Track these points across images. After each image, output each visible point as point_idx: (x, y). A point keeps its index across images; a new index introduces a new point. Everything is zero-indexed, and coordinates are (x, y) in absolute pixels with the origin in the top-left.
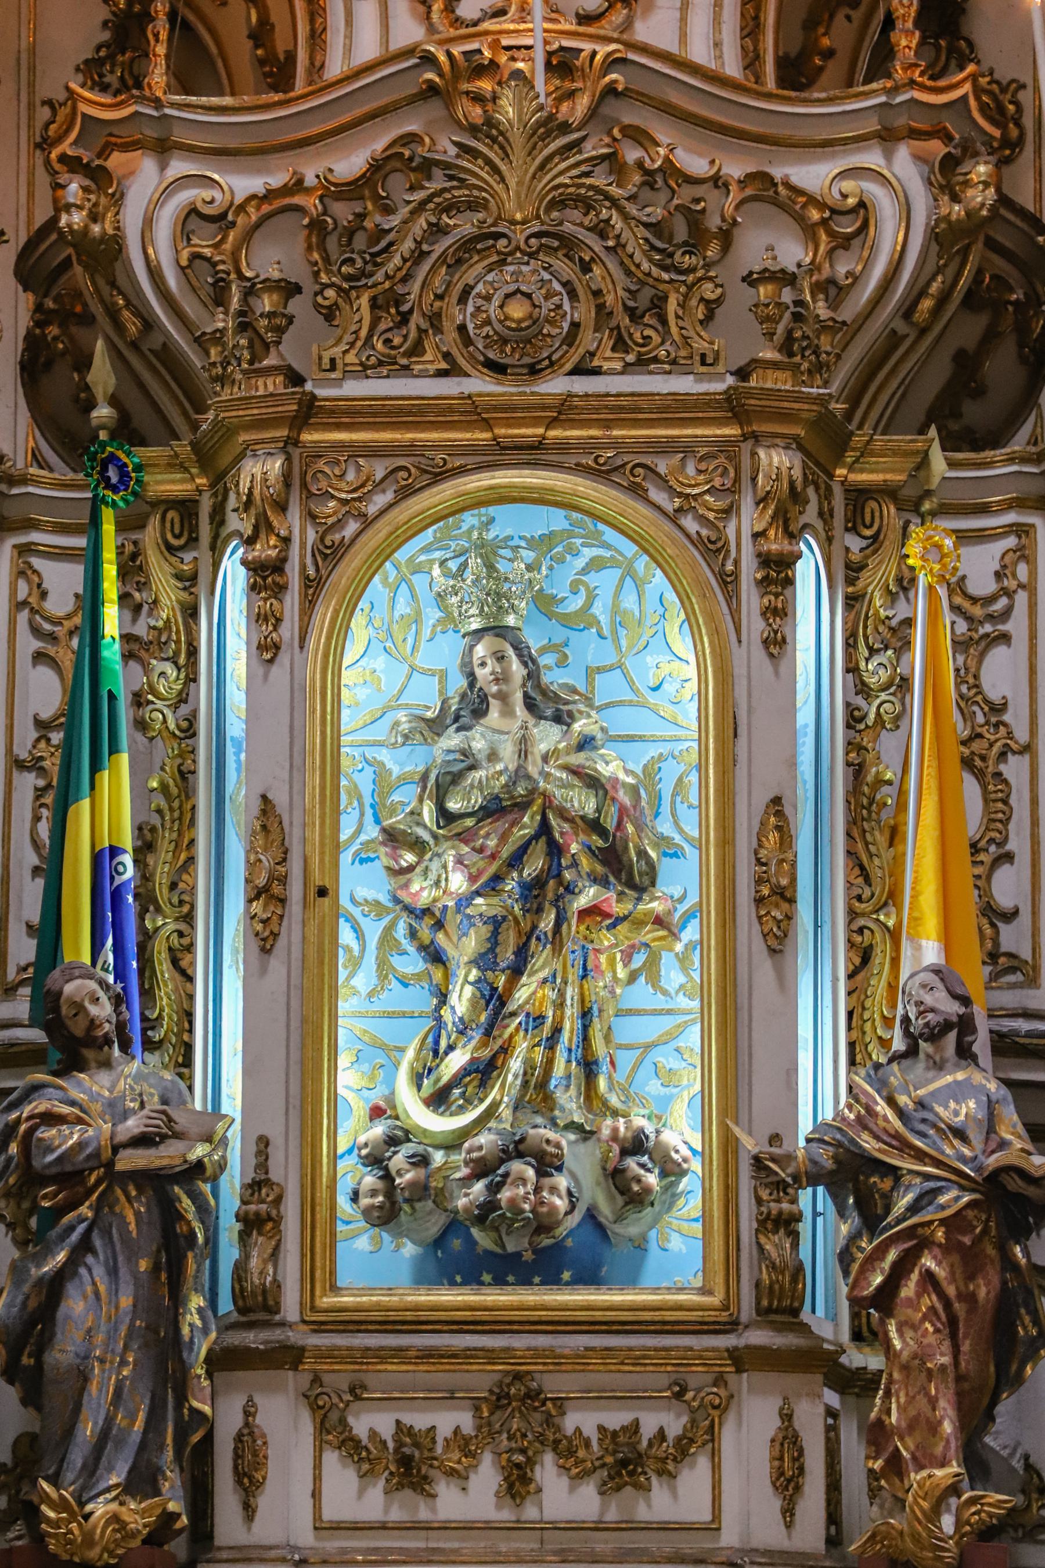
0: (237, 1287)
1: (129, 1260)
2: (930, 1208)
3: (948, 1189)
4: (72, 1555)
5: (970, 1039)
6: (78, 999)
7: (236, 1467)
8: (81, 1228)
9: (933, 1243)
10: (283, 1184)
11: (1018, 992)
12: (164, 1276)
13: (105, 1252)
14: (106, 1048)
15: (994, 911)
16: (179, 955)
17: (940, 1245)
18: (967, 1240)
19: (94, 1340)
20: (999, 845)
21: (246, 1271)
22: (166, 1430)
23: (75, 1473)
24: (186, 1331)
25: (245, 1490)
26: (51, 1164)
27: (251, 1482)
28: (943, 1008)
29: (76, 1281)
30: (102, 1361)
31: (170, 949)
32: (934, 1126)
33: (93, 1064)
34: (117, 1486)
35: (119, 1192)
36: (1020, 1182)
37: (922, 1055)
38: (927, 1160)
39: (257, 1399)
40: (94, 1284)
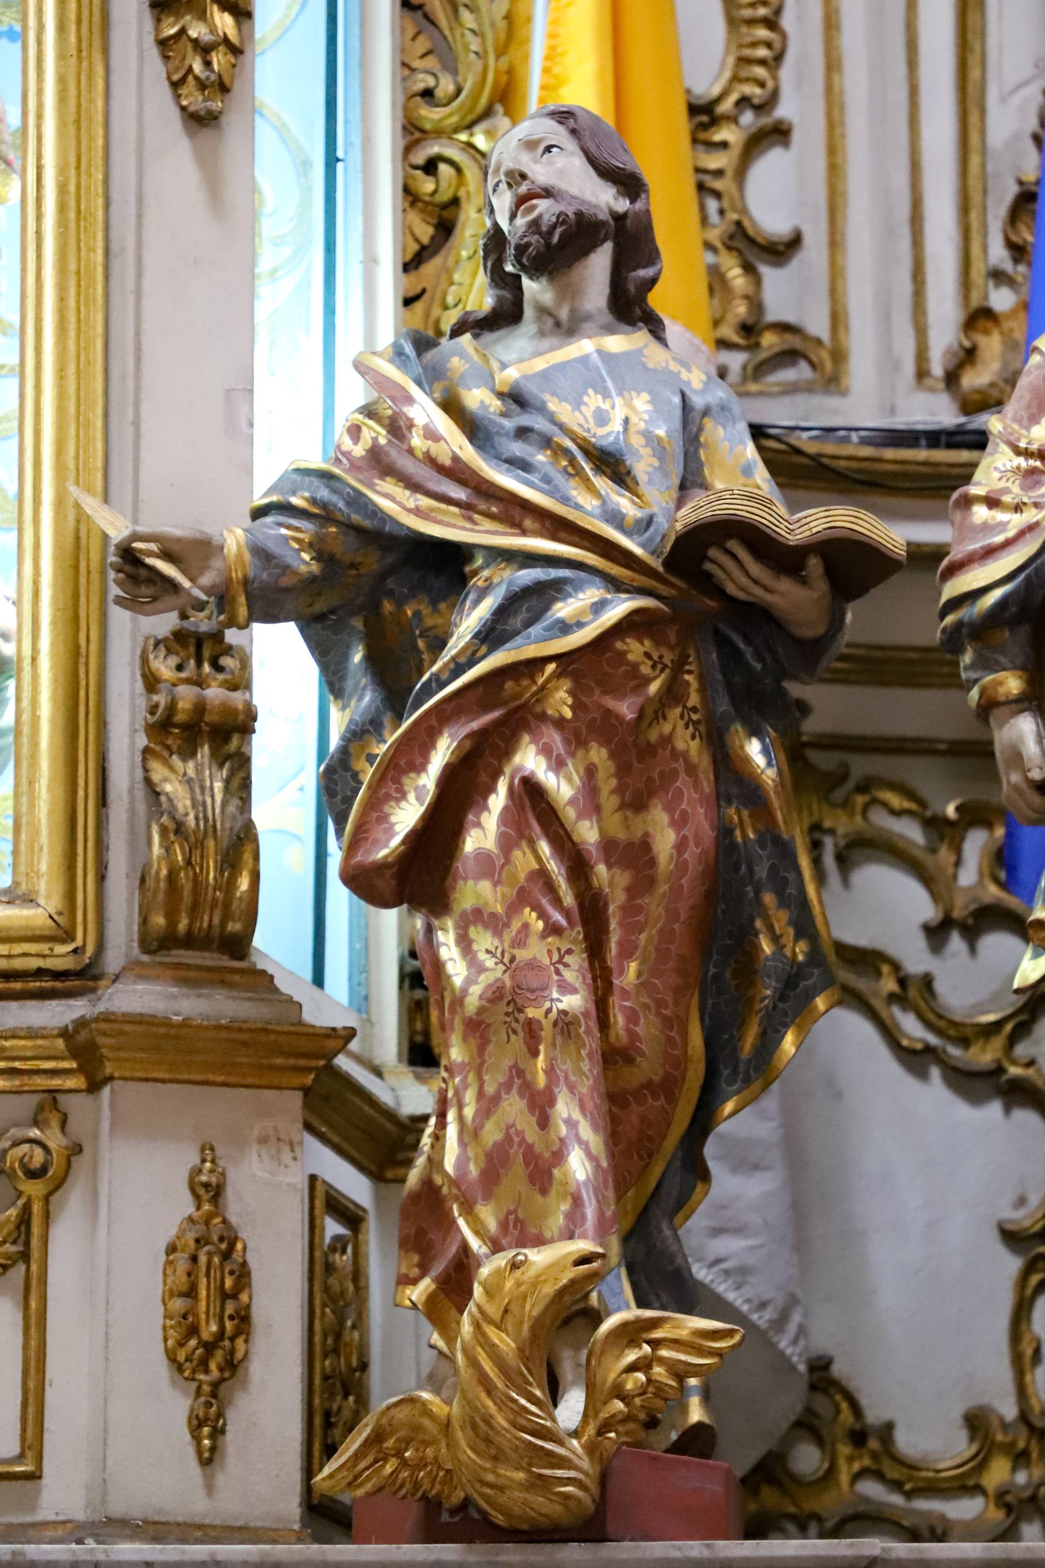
2: (535, 630)
3: (579, 587)
5: (644, 273)
9: (543, 717)
11: (800, 399)
15: (751, 241)
17: (560, 723)
18: (626, 709)
20: (763, 108)
28: (574, 191)
32: (547, 443)
36: (754, 568)
37: (528, 312)
38: (528, 523)
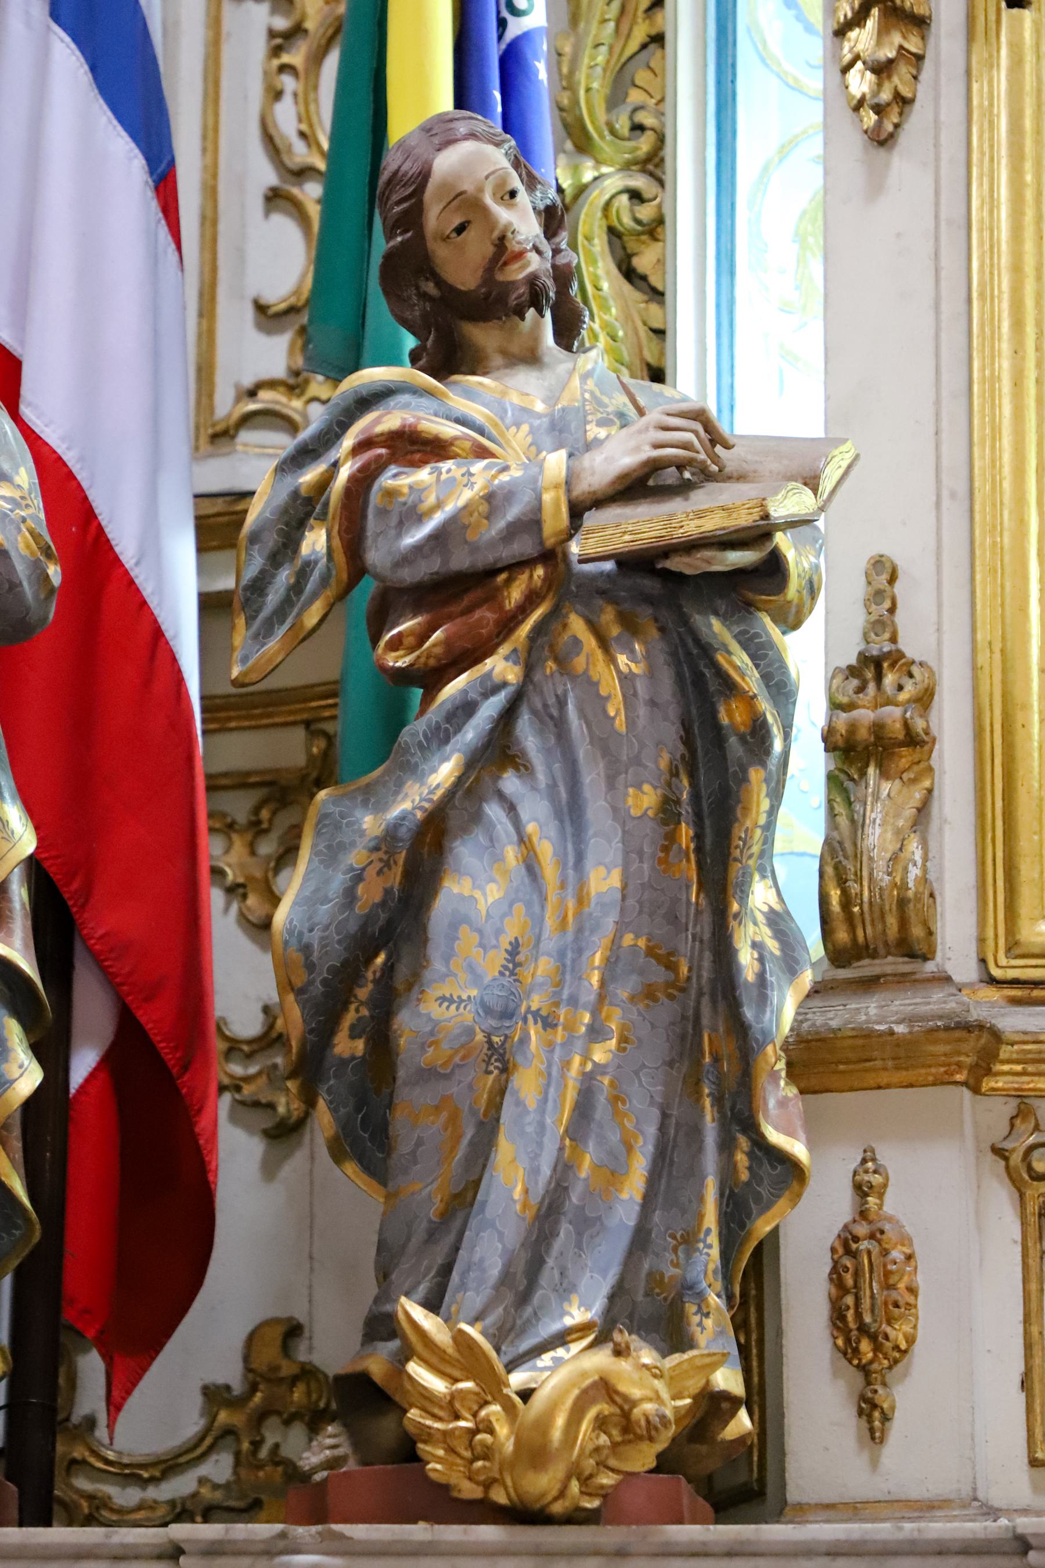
0: (835, 895)
1: (611, 782)
4: (487, 1485)
6: (468, 186)
7: (838, 1316)
8: (490, 708)
10: (932, 663)
12: (686, 832)
13: (549, 767)
14: (531, 313)
16: (631, 245)
19: (526, 974)
21: (857, 856)
22: (701, 1199)
23: (487, 1292)
24: (746, 957)
25: (864, 1369)
26: (418, 549)
27: (877, 1348)
29: (479, 836)
30: (548, 1023)
31: (612, 231)
33: (497, 360)
34: (583, 1329)
35: (577, 625)
39: (886, 1155)
40: (523, 840)
